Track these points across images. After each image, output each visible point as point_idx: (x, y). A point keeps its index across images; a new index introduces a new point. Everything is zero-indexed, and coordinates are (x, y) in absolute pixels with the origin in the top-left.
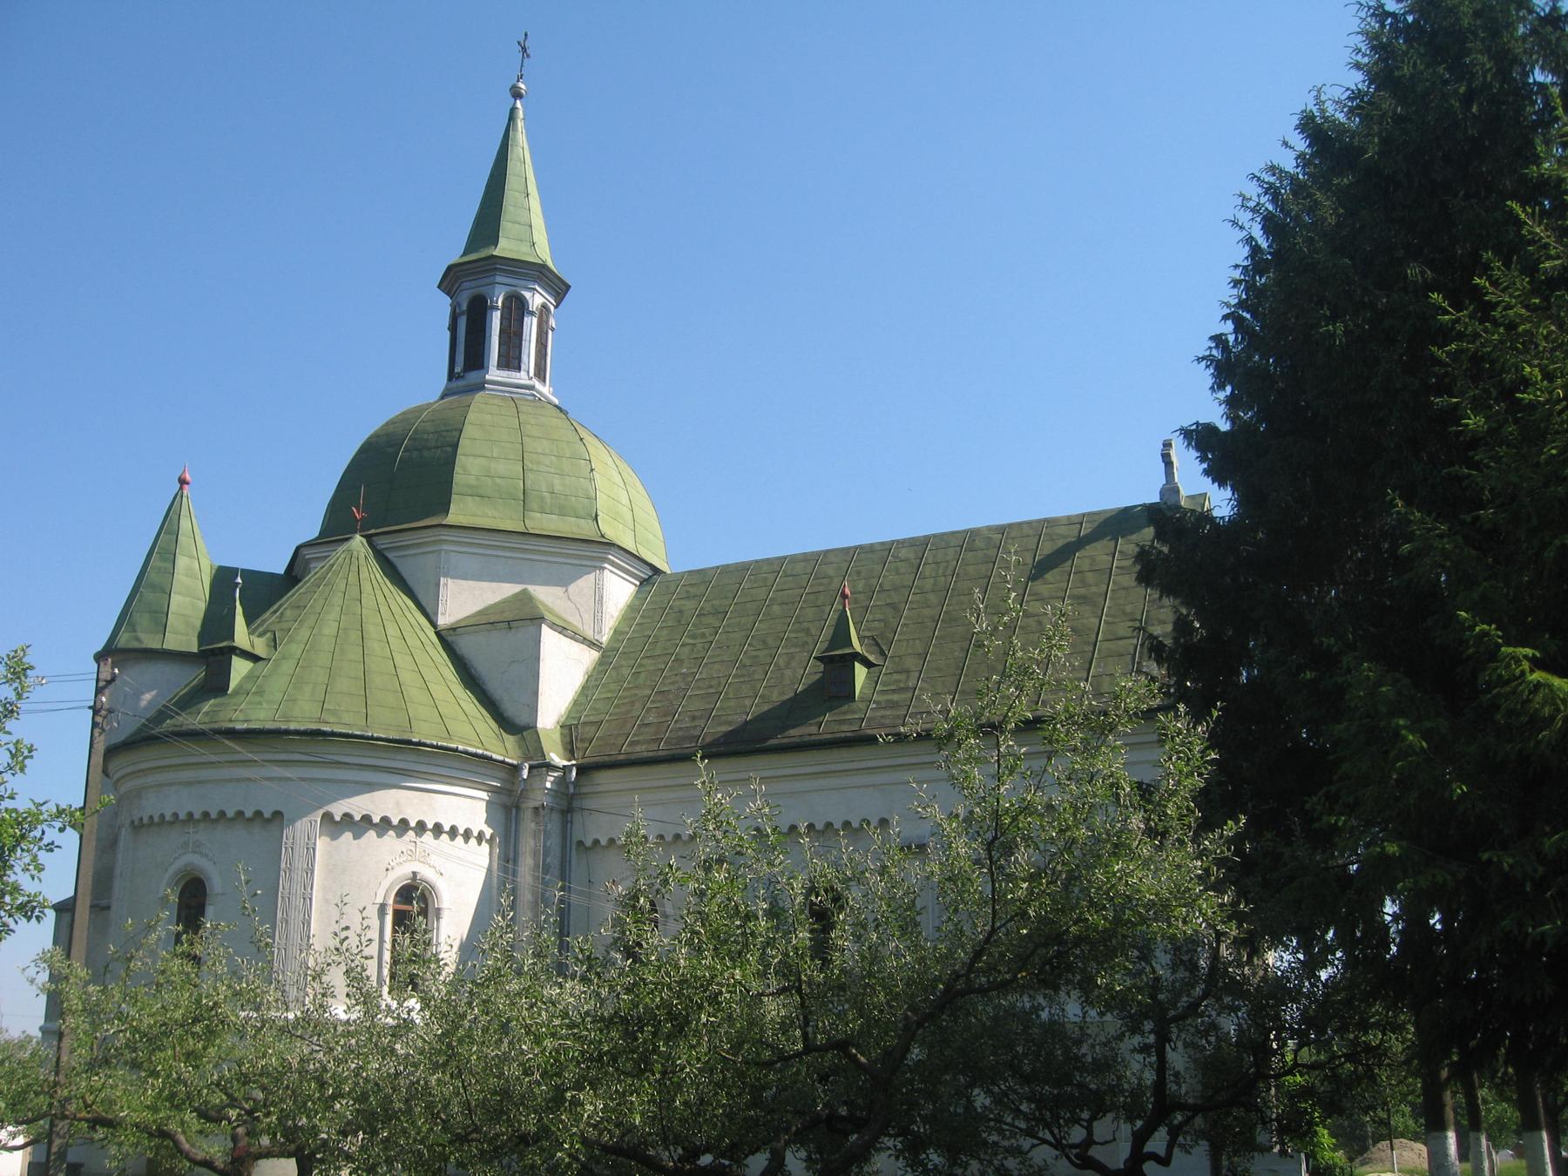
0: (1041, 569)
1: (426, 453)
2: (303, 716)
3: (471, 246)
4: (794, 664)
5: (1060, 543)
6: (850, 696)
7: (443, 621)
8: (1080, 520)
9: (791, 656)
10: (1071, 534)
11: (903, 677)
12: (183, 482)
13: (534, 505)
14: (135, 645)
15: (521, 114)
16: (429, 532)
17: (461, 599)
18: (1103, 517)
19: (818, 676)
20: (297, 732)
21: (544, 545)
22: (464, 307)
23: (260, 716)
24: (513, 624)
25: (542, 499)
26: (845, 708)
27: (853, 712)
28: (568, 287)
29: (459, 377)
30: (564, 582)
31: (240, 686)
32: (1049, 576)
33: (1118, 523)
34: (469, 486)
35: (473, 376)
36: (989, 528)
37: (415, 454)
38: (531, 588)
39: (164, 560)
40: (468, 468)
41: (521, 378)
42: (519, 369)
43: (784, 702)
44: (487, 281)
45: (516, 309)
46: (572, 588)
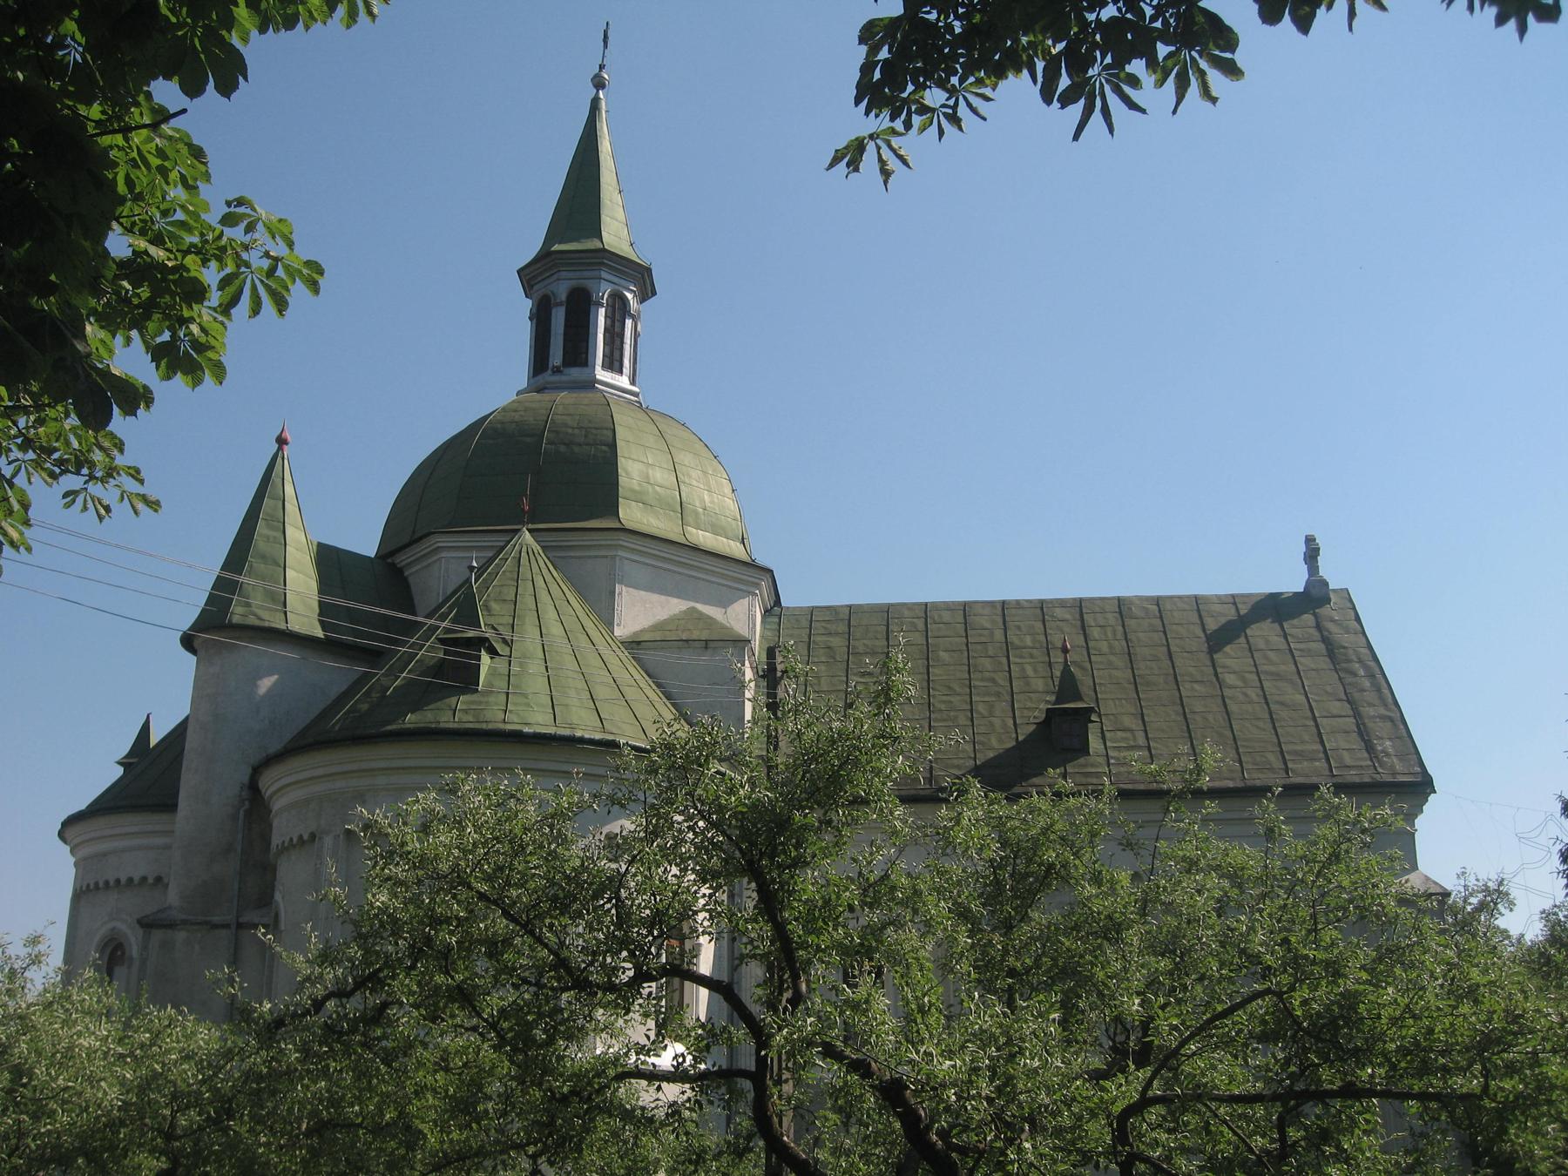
0: (1218, 640)
1: (576, 449)
2: (539, 721)
3: (554, 233)
4: (998, 713)
5: (1223, 620)
6: (1084, 750)
7: (618, 632)
8: (1234, 600)
9: (991, 707)
10: (1231, 614)
11: (1128, 735)
12: (281, 441)
13: (690, 519)
14: (252, 621)
15: (603, 104)
16: (595, 536)
17: (640, 610)
18: (1255, 599)
19: (1032, 728)
20: (591, 742)
21: (708, 563)
22: (563, 297)
23: (494, 716)
24: (711, 644)
25: (696, 513)
26: (1082, 760)
27: (1092, 766)
28: (654, 293)
29: (557, 371)
30: (724, 604)
31: (489, 684)
32: (1227, 649)
33: (1274, 608)
34: (633, 491)
35: (575, 373)
36: (1140, 598)
37: (562, 448)
38: (700, 607)
39: (269, 527)
40: (638, 467)
41: (623, 381)
42: (621, 372)
43: (1008, 750)
44: (595, 273)
45: (619, 310)
46: (729, 610)
